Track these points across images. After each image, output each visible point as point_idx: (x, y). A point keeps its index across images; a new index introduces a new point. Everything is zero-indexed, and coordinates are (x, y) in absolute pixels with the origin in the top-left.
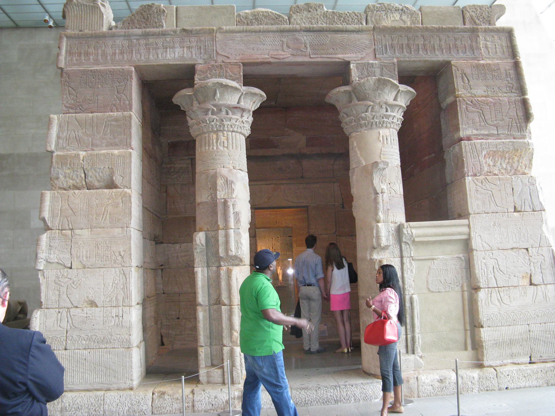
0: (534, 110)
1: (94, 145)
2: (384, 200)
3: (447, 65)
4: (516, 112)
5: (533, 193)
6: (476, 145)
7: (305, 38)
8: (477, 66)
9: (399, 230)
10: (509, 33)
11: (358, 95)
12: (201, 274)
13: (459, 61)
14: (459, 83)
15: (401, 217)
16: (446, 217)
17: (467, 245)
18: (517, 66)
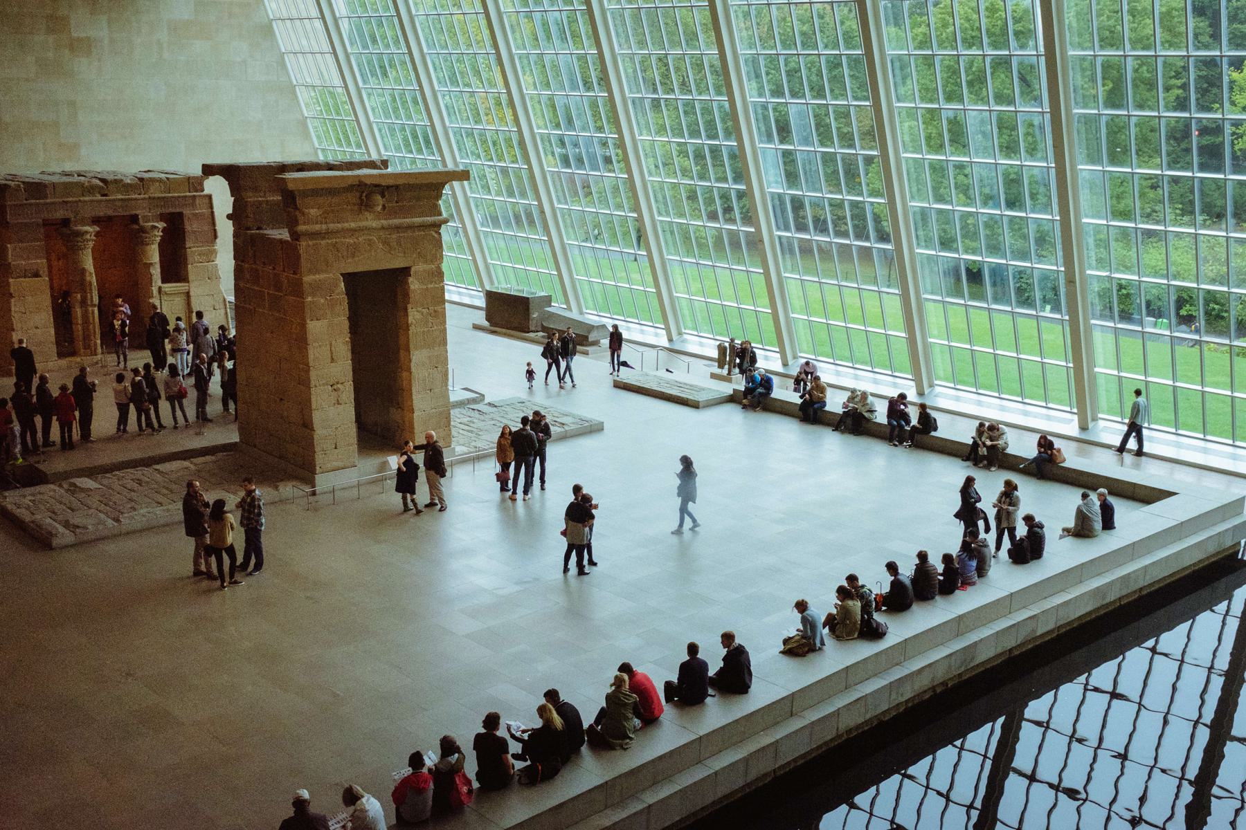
0: (219, 234)
1: (28, 258)
2: (154, 277)
3: (181, 215)
4: (210, 235)
5: (217, 271)
6: (193, 249)
7: (119, 204)
8: (195, 215)
9: (160, 288)
10: (210, 197)
11: (143, 230)
12: (78, 311)
13: (187, 212)
14: (186, 221)
15: (159, 283)
16: (178, 281)
17: (188, 294)
18: (212, 213)
